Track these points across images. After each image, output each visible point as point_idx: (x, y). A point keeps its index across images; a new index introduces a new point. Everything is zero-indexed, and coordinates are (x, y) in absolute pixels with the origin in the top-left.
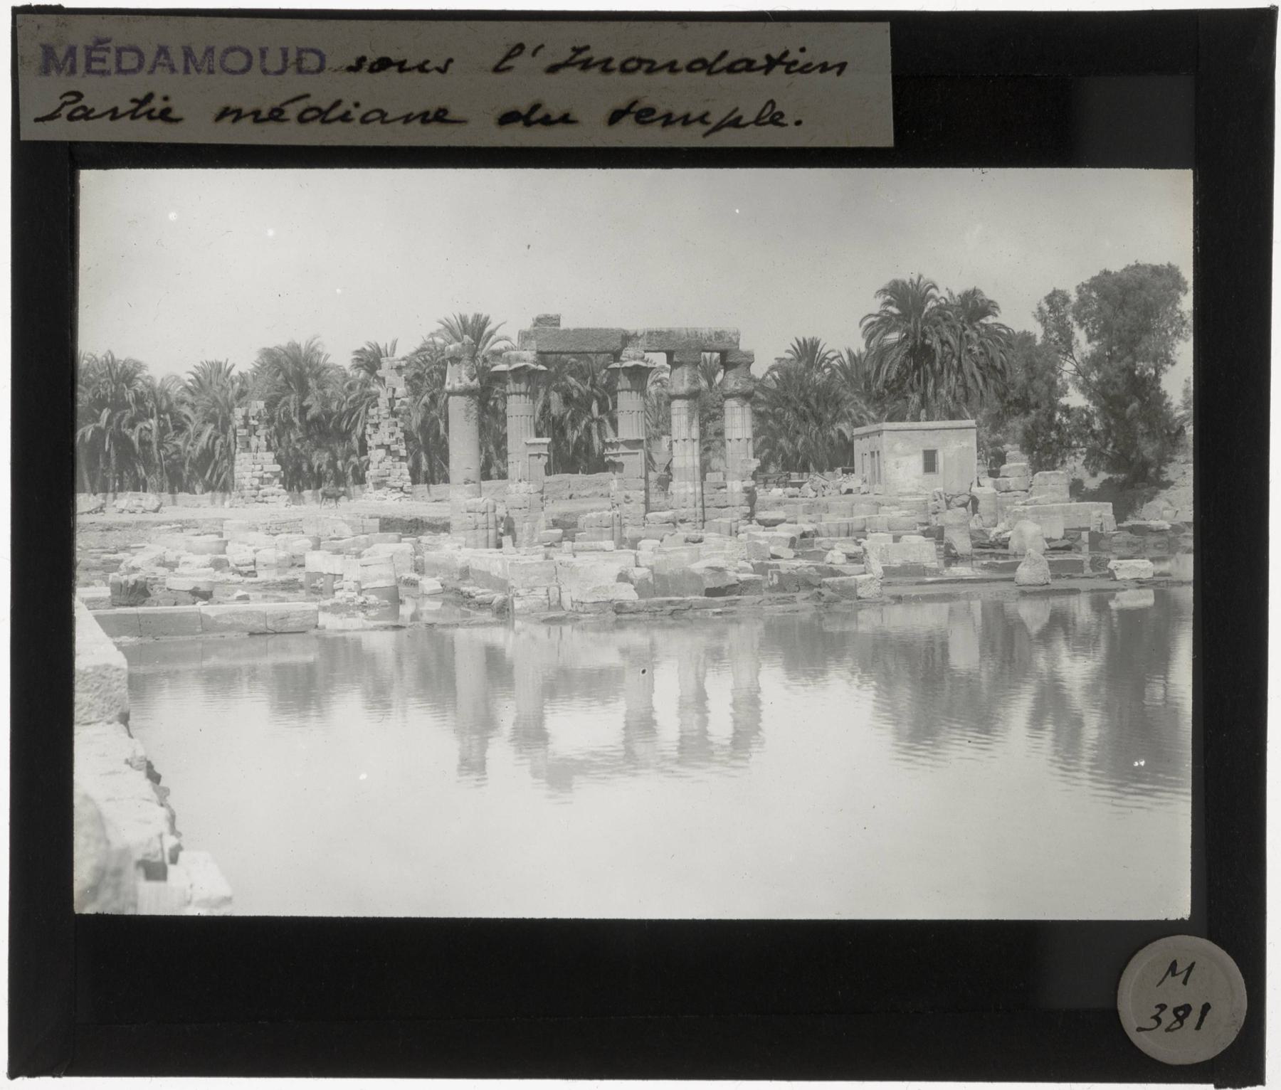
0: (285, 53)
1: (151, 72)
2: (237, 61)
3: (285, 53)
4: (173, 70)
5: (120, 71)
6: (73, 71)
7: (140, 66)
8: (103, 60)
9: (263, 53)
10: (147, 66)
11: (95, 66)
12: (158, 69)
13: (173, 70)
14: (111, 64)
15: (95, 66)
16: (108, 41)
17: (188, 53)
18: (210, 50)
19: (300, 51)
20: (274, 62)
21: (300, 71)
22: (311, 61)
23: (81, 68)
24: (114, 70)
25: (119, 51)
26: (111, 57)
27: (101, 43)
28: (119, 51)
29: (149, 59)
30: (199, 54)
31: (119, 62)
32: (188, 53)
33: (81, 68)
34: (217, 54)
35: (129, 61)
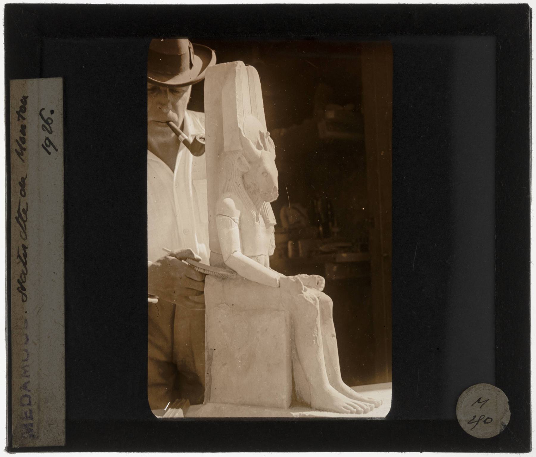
1: (29, 391)
4: (29, 382)
5: (30, 404)
6: (32, 425)
7: (26, 396)
8: (26, 413)
10: (28, 393)
11: (28, 415)
12: (28, 388)
13: (29, 382)
14: (26, 409)
15: (28, 415)
23: (30, 421)
24: (29, 407)
28: (23, 405)
29: (25, 392)
33: (30, 421)
35: (26, 401)
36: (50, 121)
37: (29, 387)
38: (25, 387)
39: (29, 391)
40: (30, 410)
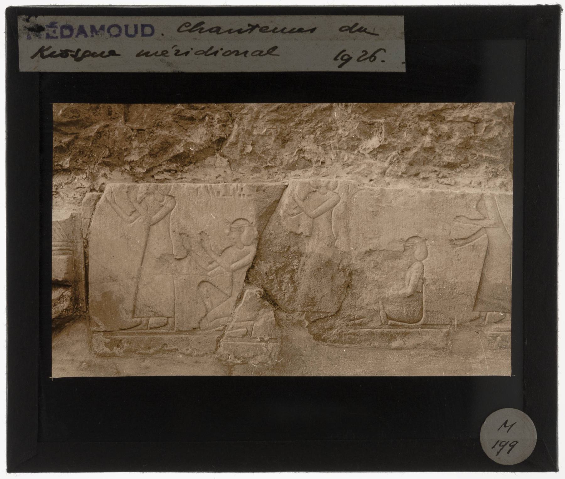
0: (136, 26)
1: (77, 36)
2: (114, 31)
3: (136, 26)
4: (86, 36)
5: (63, 36)
9: (126, 26)
12: (79, 36)
13: (86, 36)
16: (56, 23)
17: (93, 28)
18: (102, 28)
19: (143, 26)
20: (131, 31)
21: (143, 35)
22: (148, 30)
24: (59, 37)
25: (63, 27)
26: (58, 31)
27: (52, 25)
30: (98, 28)
31: (62, 32)
32: (93, 28)
34: (106, 28)
35: (67, 32)
36: (373, 58)
37: (81, 37)
38: (82, 30)
39: (77, 36)
40: (57, 37)
